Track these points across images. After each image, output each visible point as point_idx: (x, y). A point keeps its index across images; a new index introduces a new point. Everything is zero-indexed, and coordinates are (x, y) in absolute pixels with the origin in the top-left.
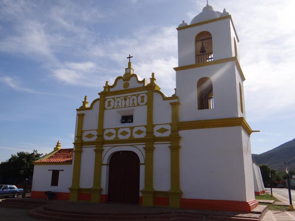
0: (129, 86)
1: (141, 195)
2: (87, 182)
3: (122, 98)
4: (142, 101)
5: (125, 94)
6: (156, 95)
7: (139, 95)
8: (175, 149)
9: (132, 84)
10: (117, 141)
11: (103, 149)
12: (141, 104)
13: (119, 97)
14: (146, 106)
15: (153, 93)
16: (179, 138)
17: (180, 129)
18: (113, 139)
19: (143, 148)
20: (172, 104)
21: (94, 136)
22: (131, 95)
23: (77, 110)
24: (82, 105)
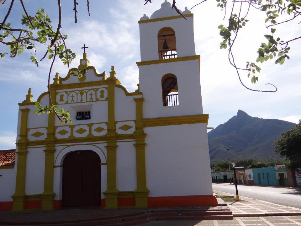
0: (85, 79)
1: (103, 197)
2: (35, 186)
3: (77, 92)
4: (102, 96)
5: (89, 86)
6: (117, 90)
7: (97, 89)
8: (140, 147)
9: (89, 77)
10: (72, 140)
11: (116, 144)
12: (100, 99)
13: (73, 91)
14: (107, 102)
15: (114, 88)
16: (144, 135)
17: (145, 126)
18: (67, 137)
19: (105, 146)
20: (136, 100)
21: (43, 134)
22: (79, 90)
23: (19, 104)
24: (25, 98)
